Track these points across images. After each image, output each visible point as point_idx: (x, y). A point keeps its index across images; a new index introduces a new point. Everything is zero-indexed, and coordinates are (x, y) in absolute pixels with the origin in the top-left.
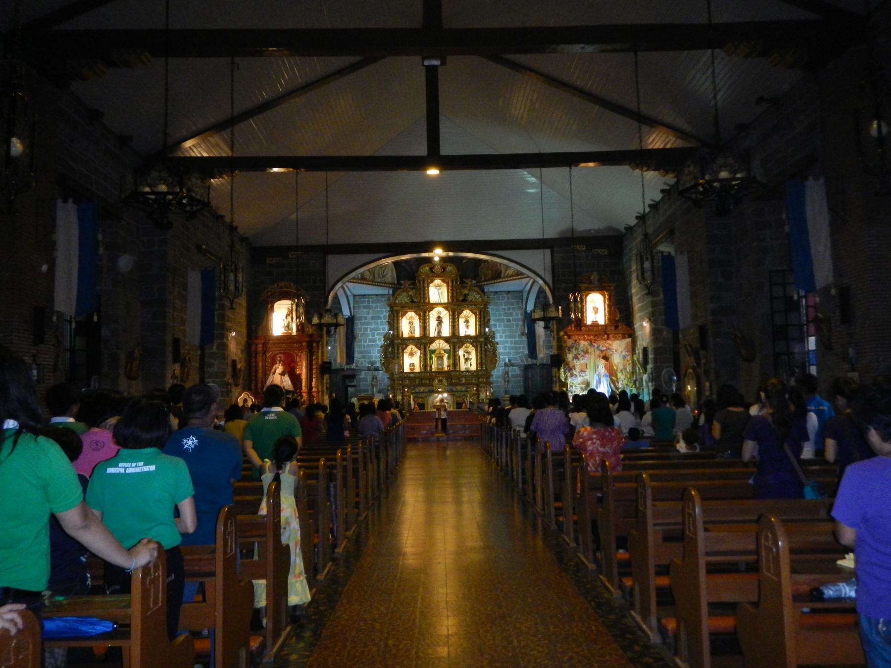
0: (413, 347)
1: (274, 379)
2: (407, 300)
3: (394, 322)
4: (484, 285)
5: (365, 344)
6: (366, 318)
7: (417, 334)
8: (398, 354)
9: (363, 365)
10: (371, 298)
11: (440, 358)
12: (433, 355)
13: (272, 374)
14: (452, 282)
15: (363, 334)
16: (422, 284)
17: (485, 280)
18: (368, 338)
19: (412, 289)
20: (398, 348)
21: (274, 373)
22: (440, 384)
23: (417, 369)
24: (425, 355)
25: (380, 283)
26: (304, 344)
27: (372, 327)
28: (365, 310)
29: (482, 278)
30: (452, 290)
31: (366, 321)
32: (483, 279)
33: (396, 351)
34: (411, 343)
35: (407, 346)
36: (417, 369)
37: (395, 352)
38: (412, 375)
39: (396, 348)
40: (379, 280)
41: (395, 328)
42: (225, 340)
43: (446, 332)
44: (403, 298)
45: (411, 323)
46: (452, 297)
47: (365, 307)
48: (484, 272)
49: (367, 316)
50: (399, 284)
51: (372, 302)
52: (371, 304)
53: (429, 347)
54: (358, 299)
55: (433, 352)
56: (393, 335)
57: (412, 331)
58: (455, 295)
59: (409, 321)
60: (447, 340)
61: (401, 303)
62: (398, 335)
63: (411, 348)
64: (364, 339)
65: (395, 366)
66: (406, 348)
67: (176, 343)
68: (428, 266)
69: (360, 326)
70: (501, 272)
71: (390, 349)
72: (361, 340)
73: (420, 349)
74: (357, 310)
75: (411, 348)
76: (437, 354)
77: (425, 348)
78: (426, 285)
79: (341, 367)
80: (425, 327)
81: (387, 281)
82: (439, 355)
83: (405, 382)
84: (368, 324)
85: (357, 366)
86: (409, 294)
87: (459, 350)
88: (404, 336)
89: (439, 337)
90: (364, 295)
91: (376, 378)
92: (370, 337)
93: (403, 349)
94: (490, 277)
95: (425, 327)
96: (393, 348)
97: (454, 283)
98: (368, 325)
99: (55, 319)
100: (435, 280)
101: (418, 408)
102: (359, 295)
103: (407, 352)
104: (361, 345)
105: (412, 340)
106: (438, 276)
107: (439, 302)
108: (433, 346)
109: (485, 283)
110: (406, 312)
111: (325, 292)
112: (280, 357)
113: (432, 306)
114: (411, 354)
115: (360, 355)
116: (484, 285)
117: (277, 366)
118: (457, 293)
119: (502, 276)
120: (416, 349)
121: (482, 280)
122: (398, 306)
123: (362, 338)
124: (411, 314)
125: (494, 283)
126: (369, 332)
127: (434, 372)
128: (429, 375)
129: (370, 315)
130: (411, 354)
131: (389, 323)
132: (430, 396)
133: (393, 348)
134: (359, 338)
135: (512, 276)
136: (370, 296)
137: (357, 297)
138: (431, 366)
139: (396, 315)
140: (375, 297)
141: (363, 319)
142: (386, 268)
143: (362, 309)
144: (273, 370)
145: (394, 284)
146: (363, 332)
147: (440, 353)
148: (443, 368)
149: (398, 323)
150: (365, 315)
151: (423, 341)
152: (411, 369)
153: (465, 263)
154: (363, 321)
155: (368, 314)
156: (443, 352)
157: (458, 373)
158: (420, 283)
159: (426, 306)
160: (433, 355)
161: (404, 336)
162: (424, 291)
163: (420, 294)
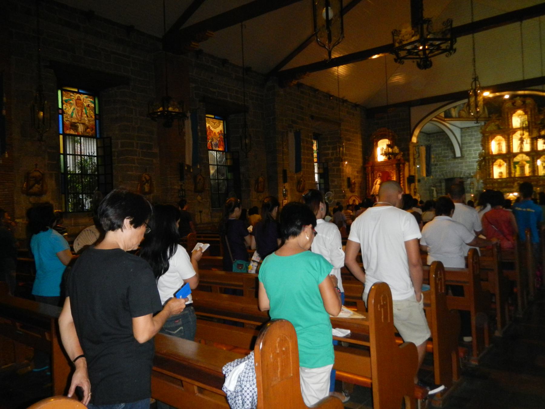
0: (501, 161)
1: (376, 188)
2: (495, 128)
5: (470, 160)
6: (470, 143)
7: (504, 150)
11: (522, 168)
12: (517, 166)
13: (374, 184)
15: (468, 154)
18: (472, 156)
19: (499, 120)
21: (376, 184)
23: (505, 176)
26: (394, 165)
27: (475, 148)
31: (470, 145)
33: (487, 164)
35: (496, 160)
36: (505, 176)
38: (499, 180)
39: (487, 162)
42: (341, 167)
43: (527, 147)
44: (492, 127)
45: (499, 144)
47: (469, 136)
50: (489, 117)
52: (473, 133)
53: (513, 160)
54: (464, 131)
55: (517, 163)
56: (485, 153)
57: (500, 150)
59: (498, 142)
60: (527, 154)
62: (489, 153)
63: (500, 161)
64: (469, 157)
66: (495, 162)
67: (285, 172)
69: (466, 149)
71: (483, 163)
72: (467, 158)
73: (506, 161)
74: (464, 138)
75: (500, 161)
76: (520, 164)
79: (454, 176)
80: (509, 146)
82: (522, 165)
84: (471, 146)
85: (465, 175)
87: (537, 161)
89: (521, 152)
90: (468, 128)
92: (474, 156)
95: (509, 146)
96: (485, 162)
98: (472, 147)
99: (186, 168)
102: (464, 128)
103: (496, 165)
104: (467, 161)
105: (500, 156)
106: (519, 108)
108: (516, 159)
111: (410, 130)
112: (379, 174)
113: (514, 131)
114: (500, 166)
117: (377, 180)
118: (535, 119)
120: (504, 162)
124: (499, 137)
126: (472, 152)
129: (473, 141)
130: (500, 166)
131: (482, 145)
133: (485, 162)
137: (464, 129)
140: (476, 127)
143: (467, 137)
144: (375, 182)
147: (522, 164)
148: (525, 174)
151: (508, 156)
152: (500, 176)
154: (468, 145)
155: (472, 140)
156: (525, 163)
157: (536, 178)
160: (517, 166)
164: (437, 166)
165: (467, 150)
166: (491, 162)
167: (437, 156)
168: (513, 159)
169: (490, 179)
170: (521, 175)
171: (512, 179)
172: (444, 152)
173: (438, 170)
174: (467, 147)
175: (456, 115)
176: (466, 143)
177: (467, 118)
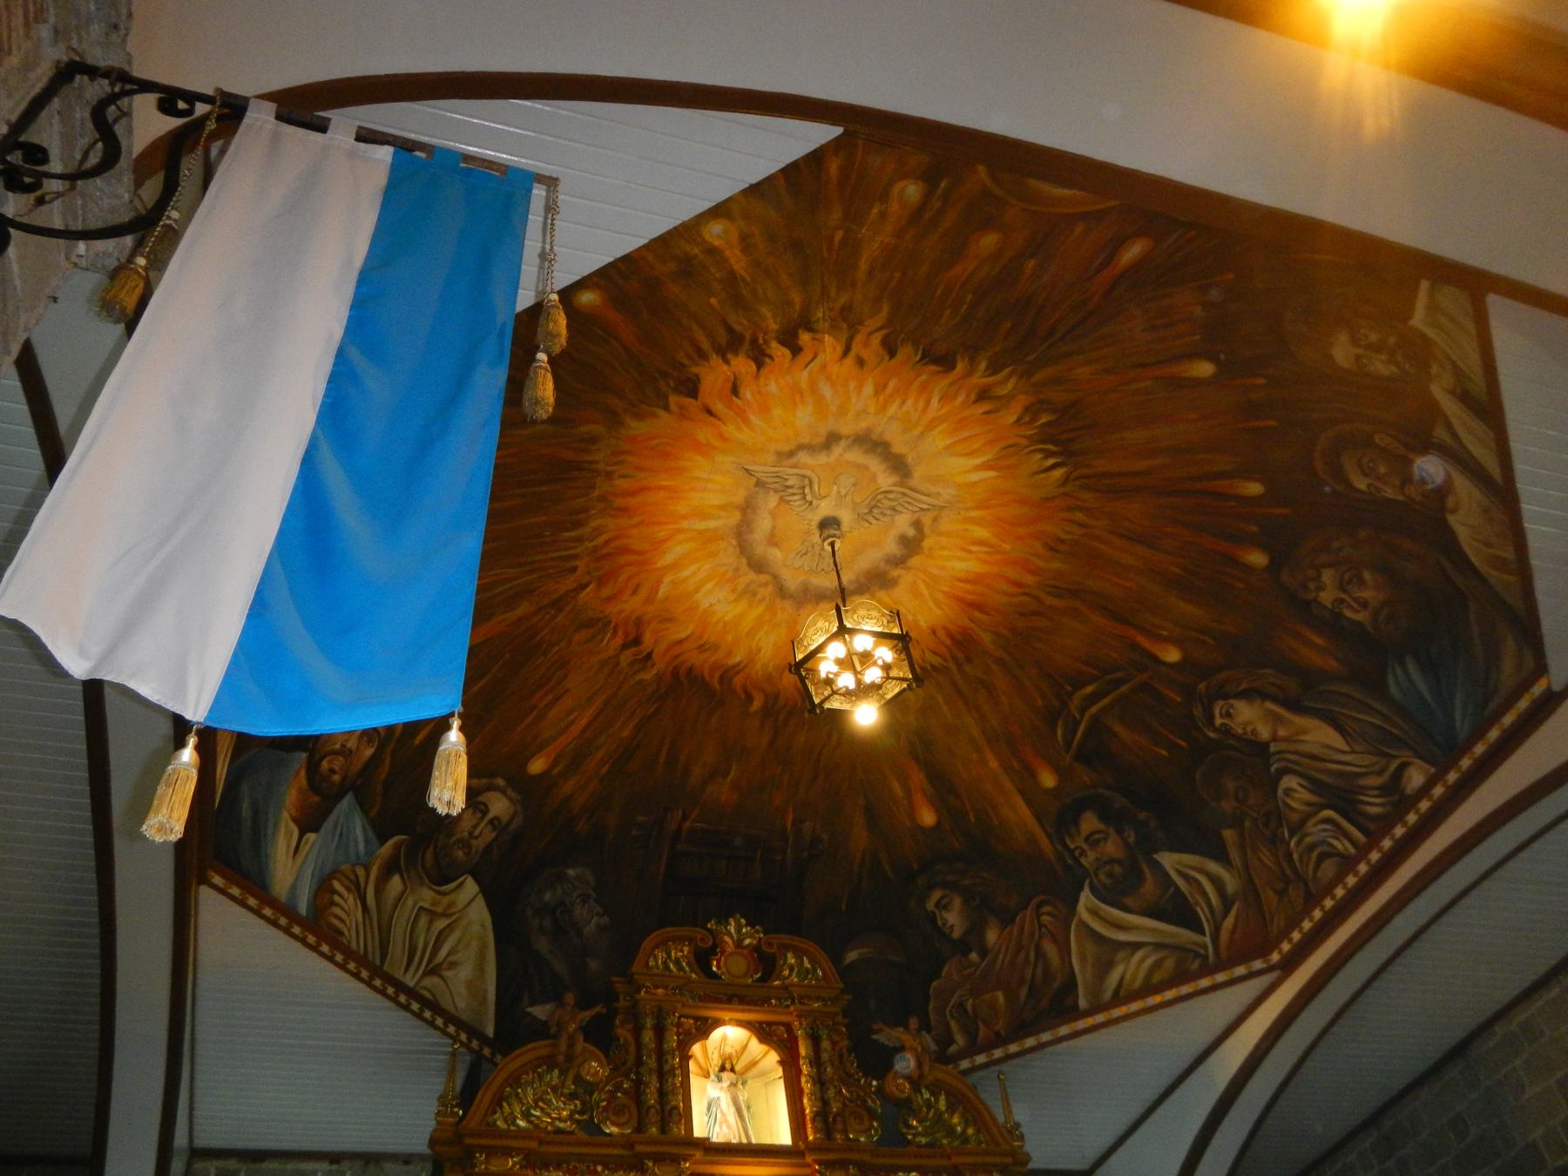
4: (975, 1069)
14: (815, 1040)
16: (648, 1036)
17: (971, 1050)
25: (412, 993)
29: (952, 1041)
30: (820, 1081)
32: (960, 1040)
40: (410, 980)
46: (822, 1114)
48: (961, 1006)
58: (835, 1107)
61: (536, 1133)
68: (681, 940)
70: (1070, 985)
78: (672, 1040)
81: (446, 1003)
86: (578, 1079)
94: (1000, 1026)
97: (825, 1044)
100: (718, 1023)
106: (734, 997)
107: (744, 1141)
109: (981, 1059)
116: (975, 1069)
119: (1083, 1003)
121: (953, 1049)
122: (508, 1152)
125: (1041, 1046)
135: (1149, 989)
142: (450, 928)
145: (484, 1040)
153: (852, 963)
158: (637, 1032)
162: (662, 1075)
163: (637, 1094)
175: (294, 887)
177: (362, 961)
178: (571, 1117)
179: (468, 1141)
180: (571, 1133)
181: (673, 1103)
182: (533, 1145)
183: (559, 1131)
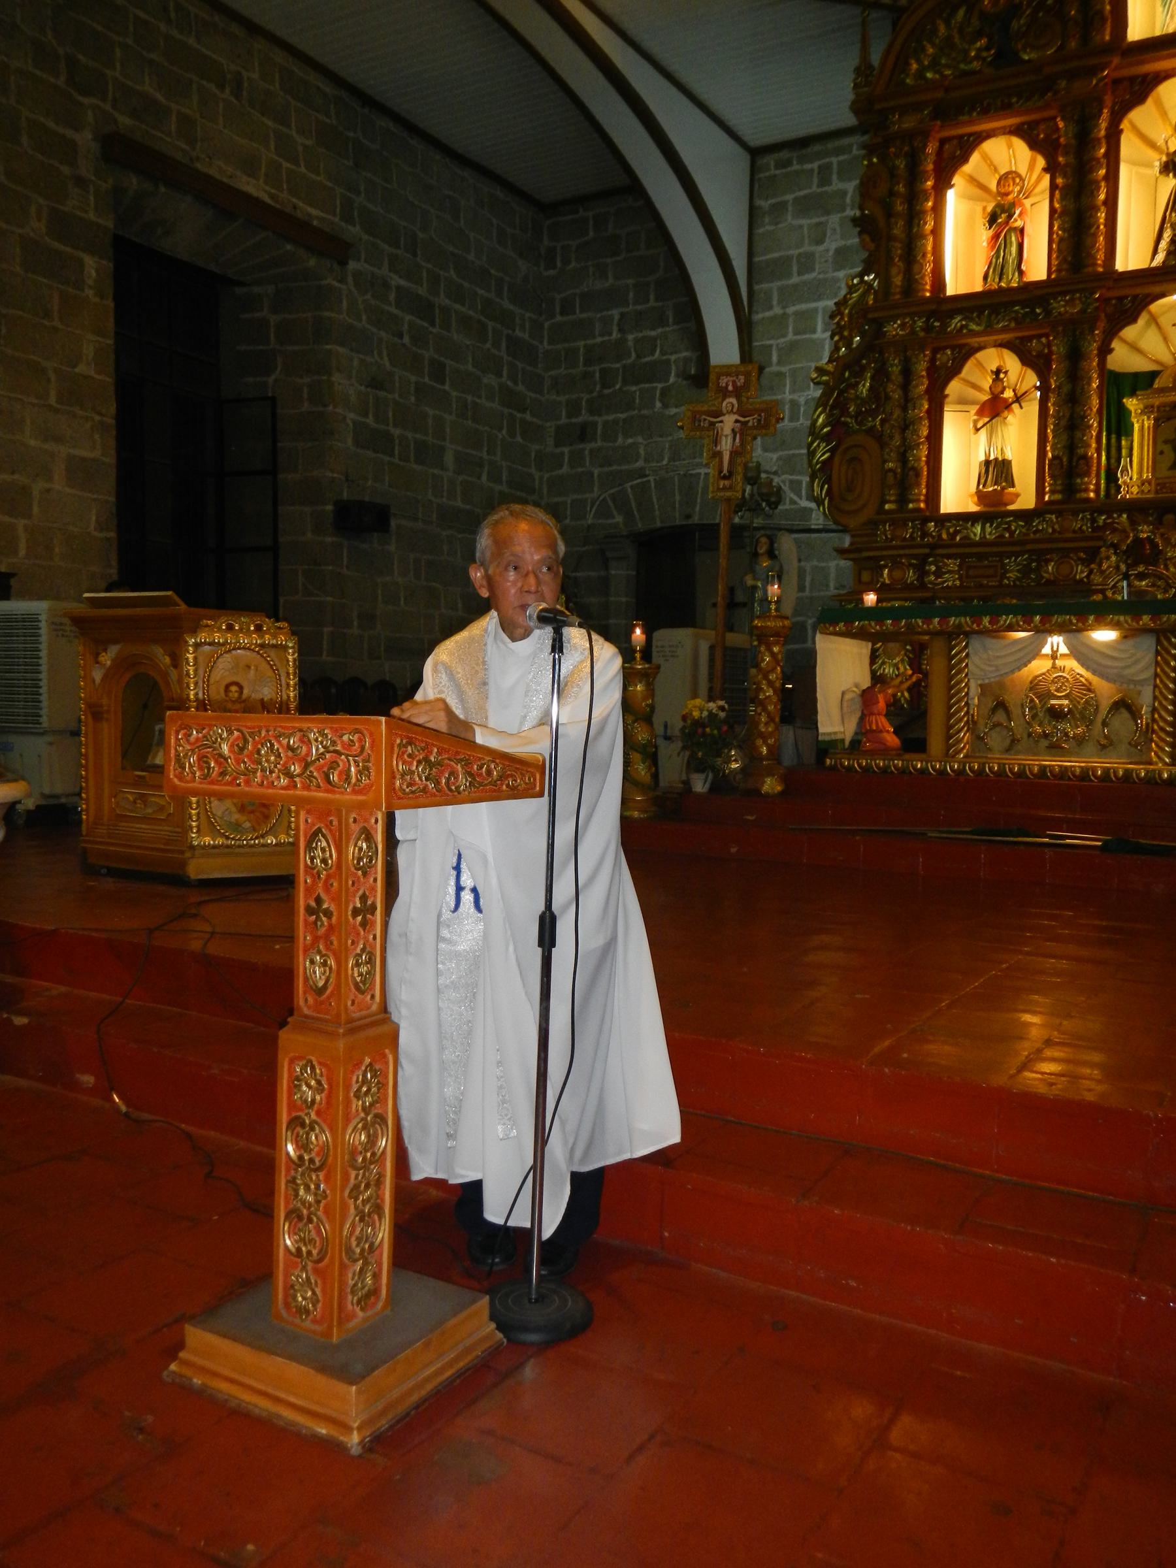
0: (1012, 363)
3: (889, 214)
7: (1037, 267)
8: (904, 409)
9: (787, 506)
10: (839, 151)
12: (1131, 403)
15: (793, 346)
20: (907, 373)
22: (1141, 576)
23: (1025, 496)
24: (1073, 399)
28: (805, 222)
34: (989, 330)
35: (965, 354)
37: (888, 398)
39: (895, 369)
41: (898, 250)
47: (805, 206)
49: (813, 248)
51: (841, 178)
52: (836, 185)
55: (1142, 382)
59: (989, 209)
64: (794, 372)
65: (718, 414)
66: (954, 371)
69: (777, 310)
72: (780, 375)
76: (1162, 390)
77: (1075, 356)
79: (688, 517)
83: (938, 573)
84: (816, 291)
88: (950, 291)
91: (771, 554)
93: (940, 378)
96: (881, 375)
101: (892, 740)
110: (965, 148)
115: (775, 456)
123: (784, 369)
127: (1136, 508)
128: (1087, 528)
129: (832, 244)
131: (863, 224)
132: (976, 643)
133: (881, 375)
134: (775, 368)
136: (830, 145)
137: (770, 160)
138: (1112, 477)
139: (901, 164)
141: (795, 269)
143: (790, 219)
146: (790, 336)
149: (914, 216)
150: (807, 248)
151: (1060, 306)
152: (981, 496)
154: (795, 279)
155: (820, 241)
159: (1094, 70)
161: (950, 291)
164: (594, 439)
165: (785, 316)
166: (921, 367)
167: (596, 369)
168: (1112, 332)
169: (900, 518)
170: (1161, 486)
171: (1080, 523)
172: (637, 341)
173: (596, 472)
174: (788, 295)
176: (781, 268)
178: (977, 57)
179: (878, 107)
180: (979, 72)
181: (1098, 7)
182: (939, 94)
183: (965, 74)
